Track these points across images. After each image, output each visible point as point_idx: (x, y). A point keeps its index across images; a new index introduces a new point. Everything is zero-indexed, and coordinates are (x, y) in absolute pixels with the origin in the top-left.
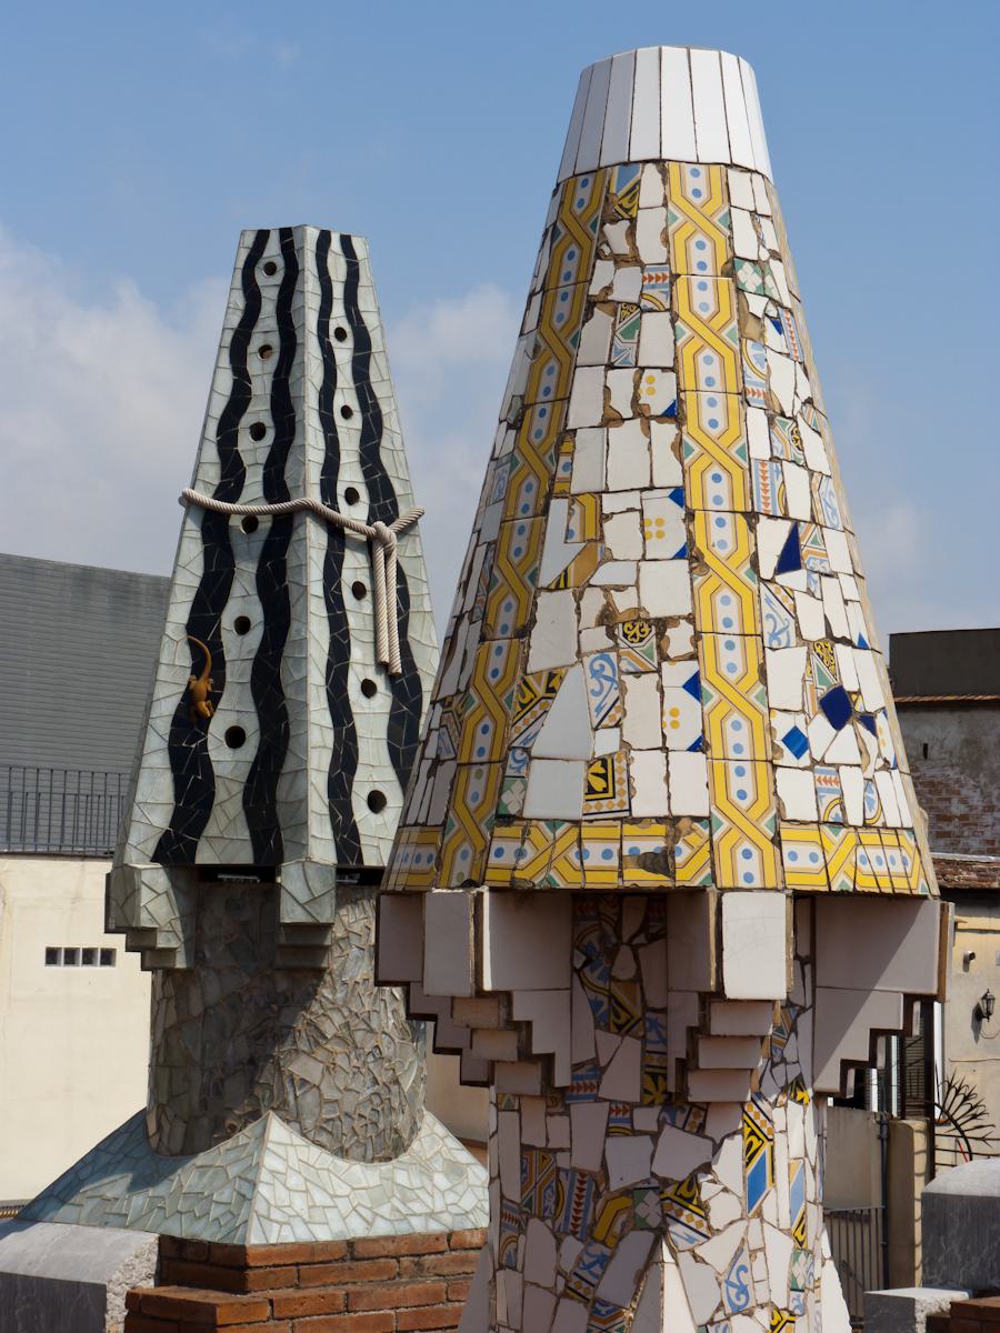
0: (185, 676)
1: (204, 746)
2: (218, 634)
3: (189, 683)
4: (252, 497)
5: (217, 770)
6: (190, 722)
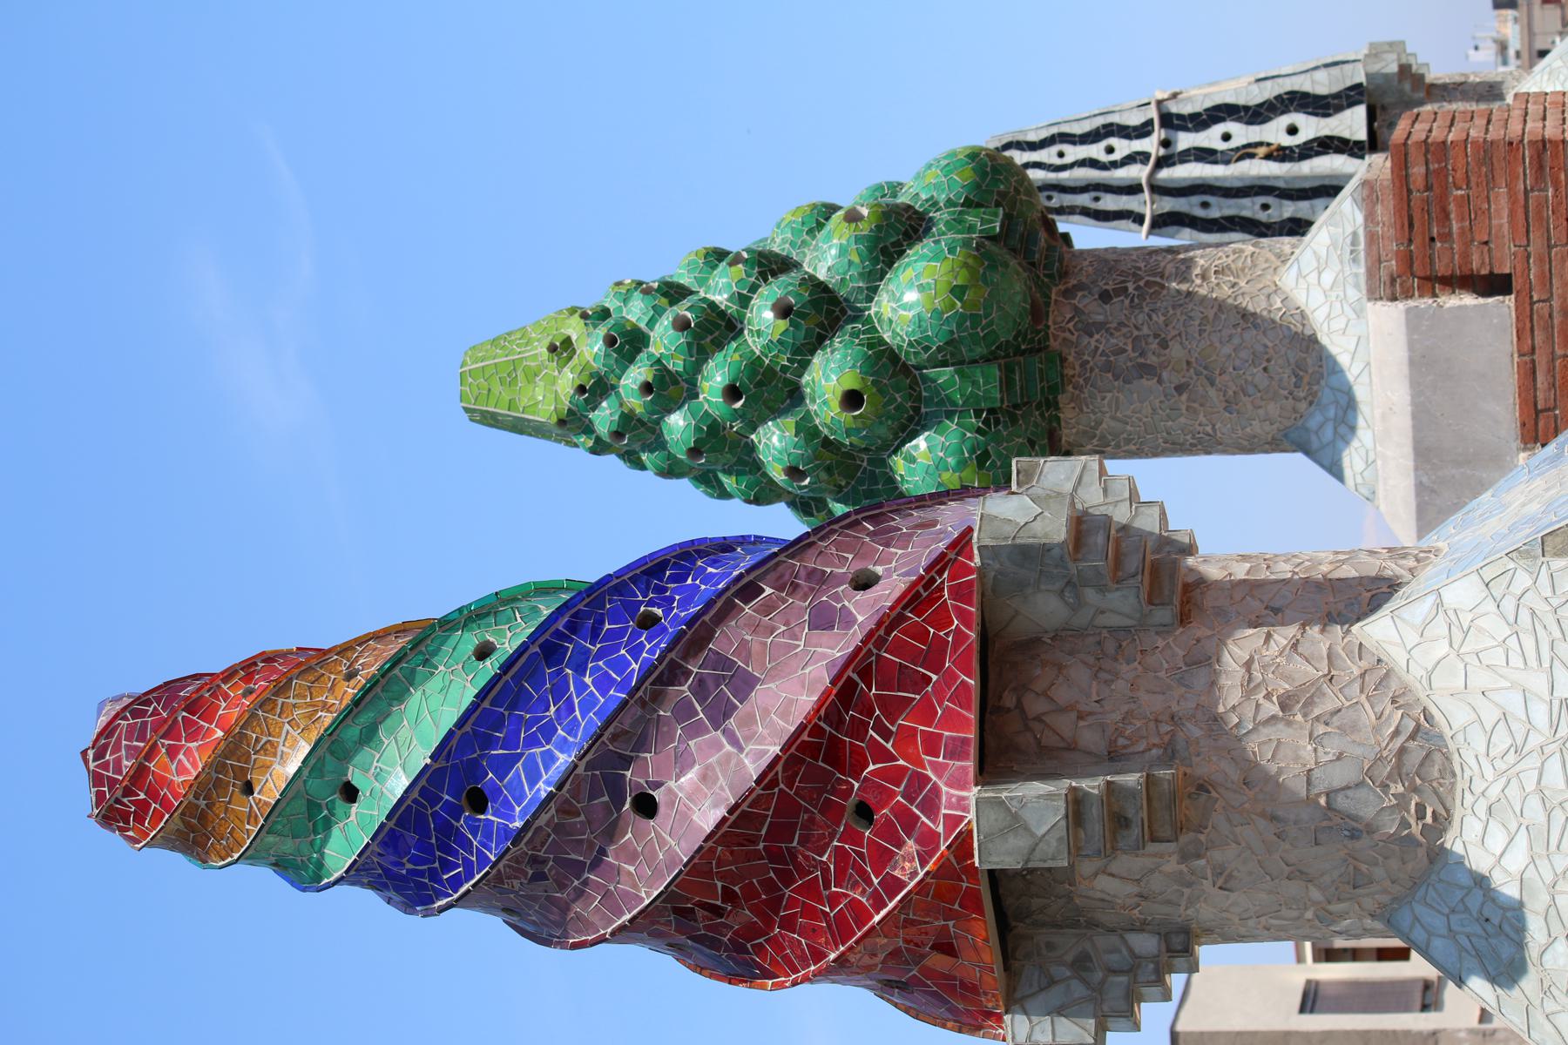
0: (1256, 162)
1: (1298, 146)
2: (1232, 150)
3: (1261, 158)
4: (1150, 145)
5: (1311, 136)
6: (1281, 154)
